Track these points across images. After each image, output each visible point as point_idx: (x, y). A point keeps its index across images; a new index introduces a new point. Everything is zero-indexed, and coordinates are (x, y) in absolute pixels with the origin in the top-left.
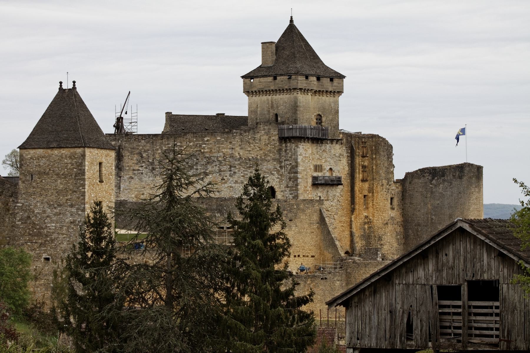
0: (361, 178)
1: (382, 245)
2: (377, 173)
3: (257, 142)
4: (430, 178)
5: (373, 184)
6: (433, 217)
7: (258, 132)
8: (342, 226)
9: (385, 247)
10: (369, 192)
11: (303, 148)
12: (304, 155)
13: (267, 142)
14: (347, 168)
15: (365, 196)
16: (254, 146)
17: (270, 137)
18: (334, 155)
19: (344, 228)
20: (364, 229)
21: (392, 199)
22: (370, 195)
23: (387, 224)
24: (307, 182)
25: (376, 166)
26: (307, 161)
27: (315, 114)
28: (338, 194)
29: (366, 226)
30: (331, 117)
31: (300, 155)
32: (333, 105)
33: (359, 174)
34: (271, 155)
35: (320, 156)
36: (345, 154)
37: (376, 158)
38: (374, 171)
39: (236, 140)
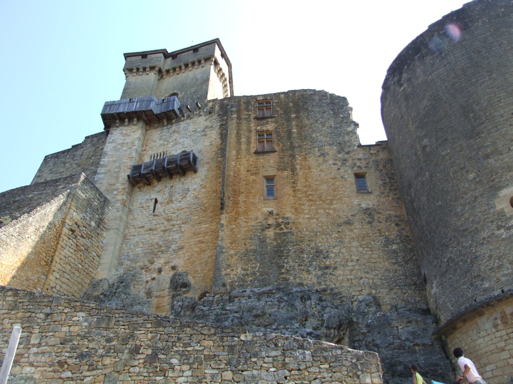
0: (253, 150)
1: (327, 267)
2: (303, 138)
3: (77, 158)
4: (396, 79)
5: (293, 156)
6: (426, 141)
7: (82, 148)
8: (201, 242)
9: (339, 272)
10: (281, 168)
11: (121, 133)
12: (121, 142)
13: (92, 154)
14: (219, 141)
15: (270, 179)
16: (71, 164)
17: (98, 147)
18: (193, 131)
19: (203, 245)
20: (263, 241)
21: (359, 176)
22: (286, 173)
23: (348, 223)
24: (117, 178)
25: (301, 127)
26: (125, 148)
27: (167, 95)
28: (195, 186)
29: (270, 233)
30: (193, 90)
31: (109, 143)
32: (199, 77)
33: (249, 143)
34: (92, 168)
35: (164, 140)
36: (217, 125)
37: (297, 117)
38: (295, 135)
39: (48, 165)
